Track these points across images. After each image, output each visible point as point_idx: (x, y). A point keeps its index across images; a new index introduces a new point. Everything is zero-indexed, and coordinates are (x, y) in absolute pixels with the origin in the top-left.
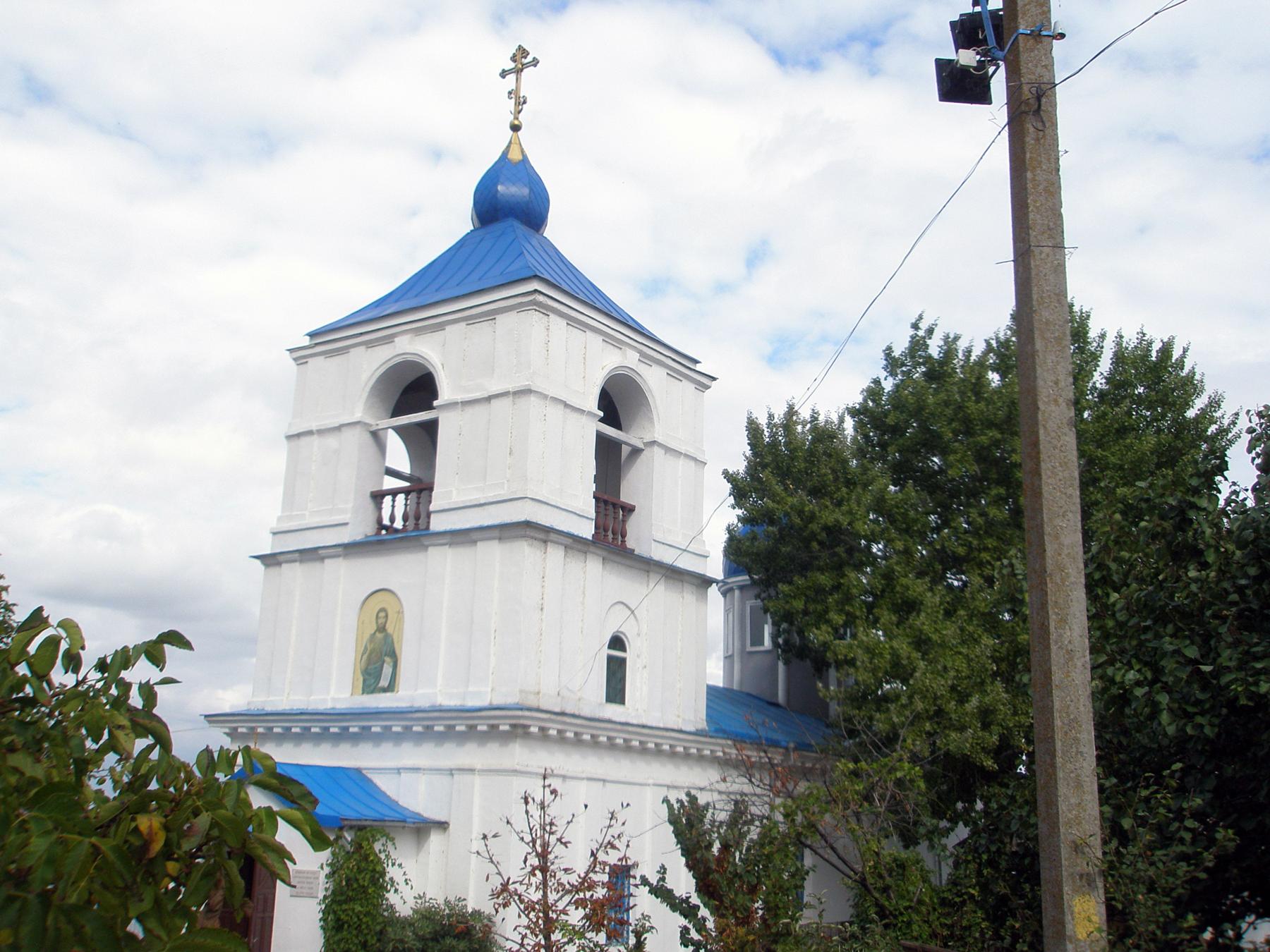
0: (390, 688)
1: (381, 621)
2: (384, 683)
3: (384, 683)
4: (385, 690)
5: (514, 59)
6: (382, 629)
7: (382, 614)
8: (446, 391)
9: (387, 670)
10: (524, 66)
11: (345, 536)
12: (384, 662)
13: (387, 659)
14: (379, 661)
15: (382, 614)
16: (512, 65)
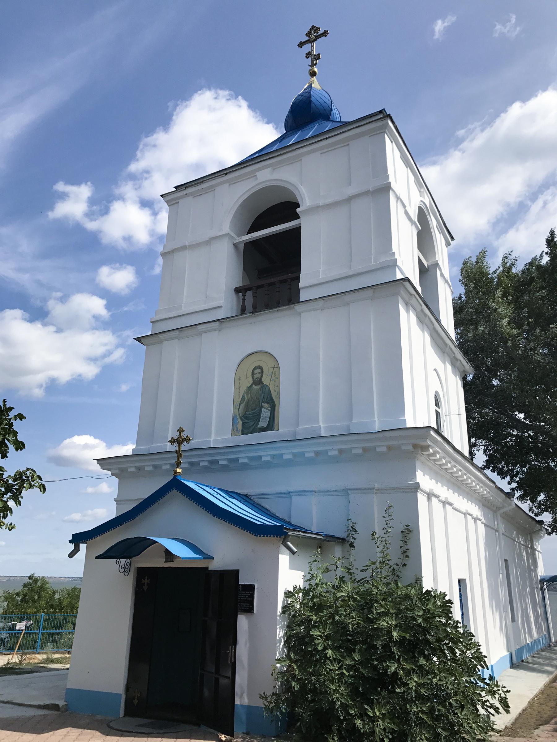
0: (270, 427)
1: (256, 376)
2: (263, 424)
3: (263, 424)
4: (263, 430)
5: (309, 34)
6: (258, 382)
7: (258, 371)
8: (306, 201)
9: (266, 413)
10: (317, 37)
11: (220, 314)
12: (262, 407)
13: (266, 405)
14: (257, 408)
15: (258, 371)
16: (308, 38)
